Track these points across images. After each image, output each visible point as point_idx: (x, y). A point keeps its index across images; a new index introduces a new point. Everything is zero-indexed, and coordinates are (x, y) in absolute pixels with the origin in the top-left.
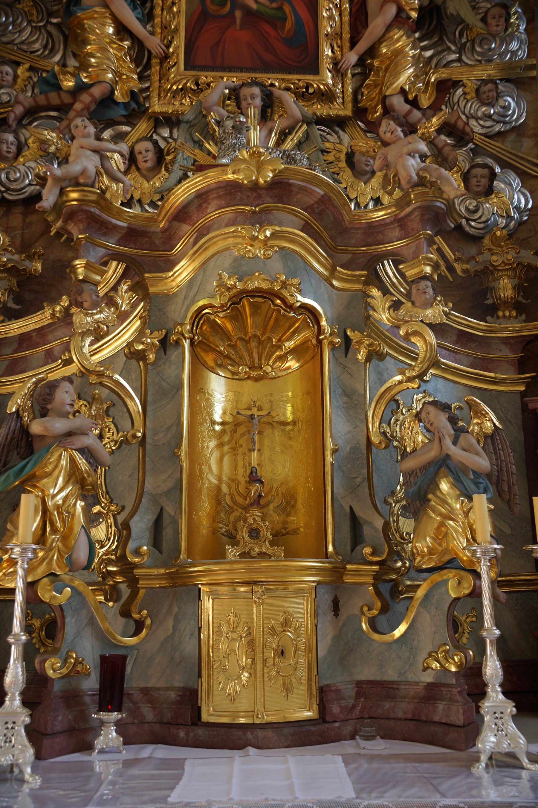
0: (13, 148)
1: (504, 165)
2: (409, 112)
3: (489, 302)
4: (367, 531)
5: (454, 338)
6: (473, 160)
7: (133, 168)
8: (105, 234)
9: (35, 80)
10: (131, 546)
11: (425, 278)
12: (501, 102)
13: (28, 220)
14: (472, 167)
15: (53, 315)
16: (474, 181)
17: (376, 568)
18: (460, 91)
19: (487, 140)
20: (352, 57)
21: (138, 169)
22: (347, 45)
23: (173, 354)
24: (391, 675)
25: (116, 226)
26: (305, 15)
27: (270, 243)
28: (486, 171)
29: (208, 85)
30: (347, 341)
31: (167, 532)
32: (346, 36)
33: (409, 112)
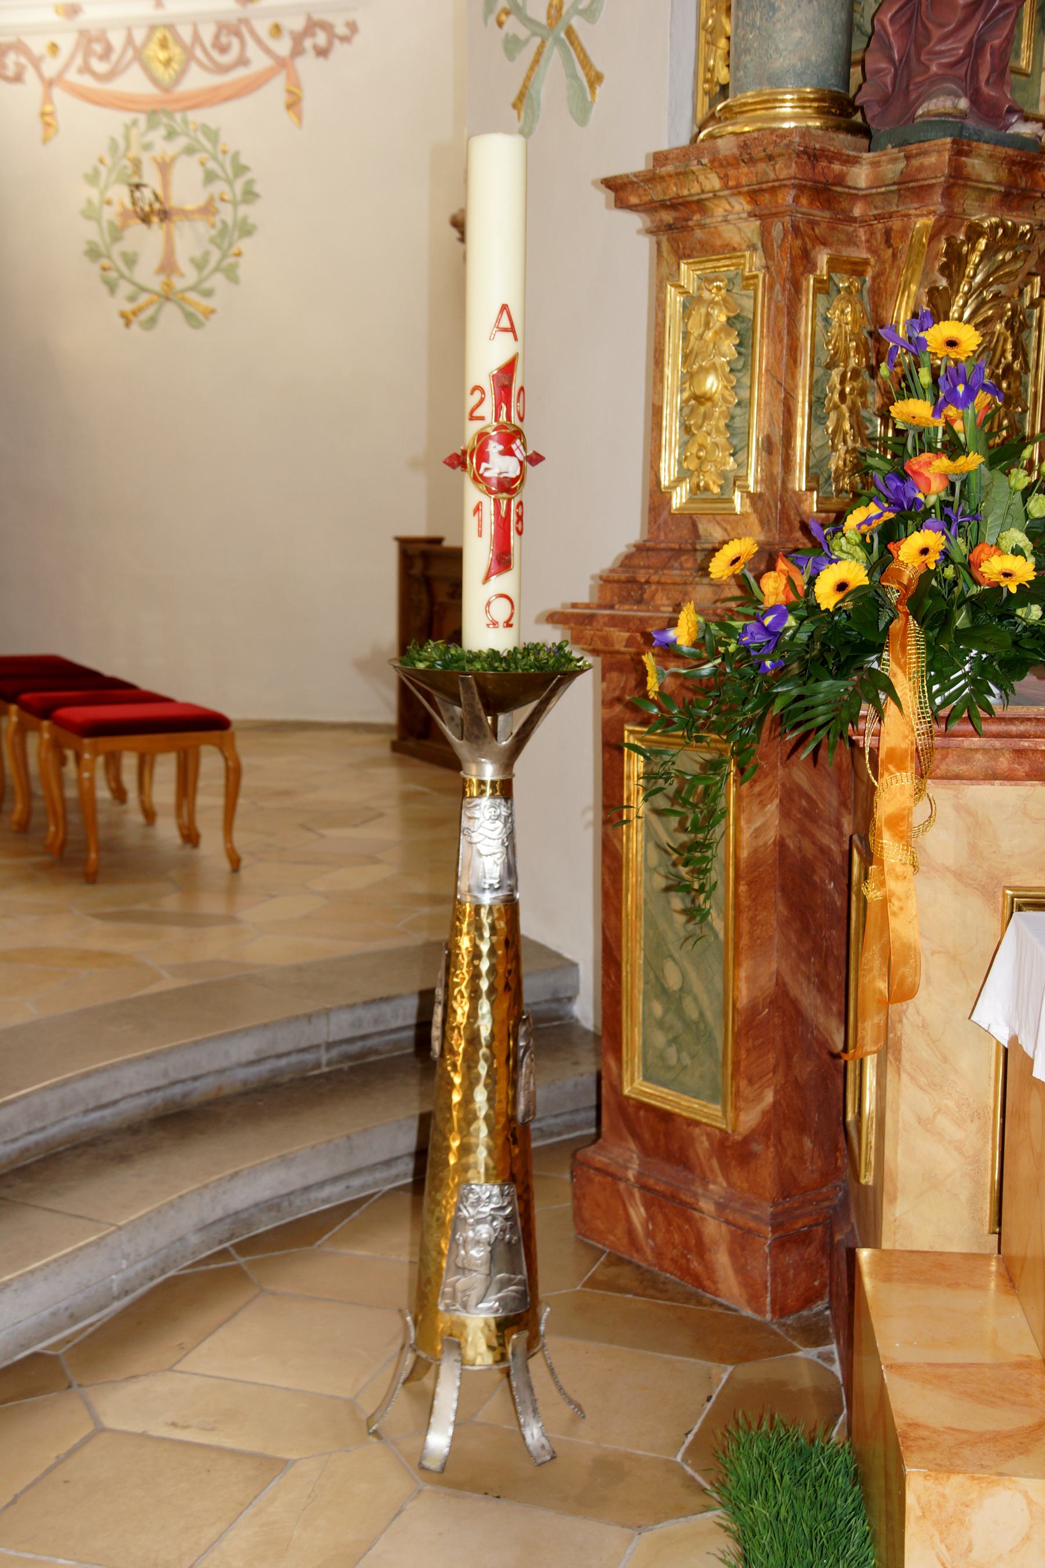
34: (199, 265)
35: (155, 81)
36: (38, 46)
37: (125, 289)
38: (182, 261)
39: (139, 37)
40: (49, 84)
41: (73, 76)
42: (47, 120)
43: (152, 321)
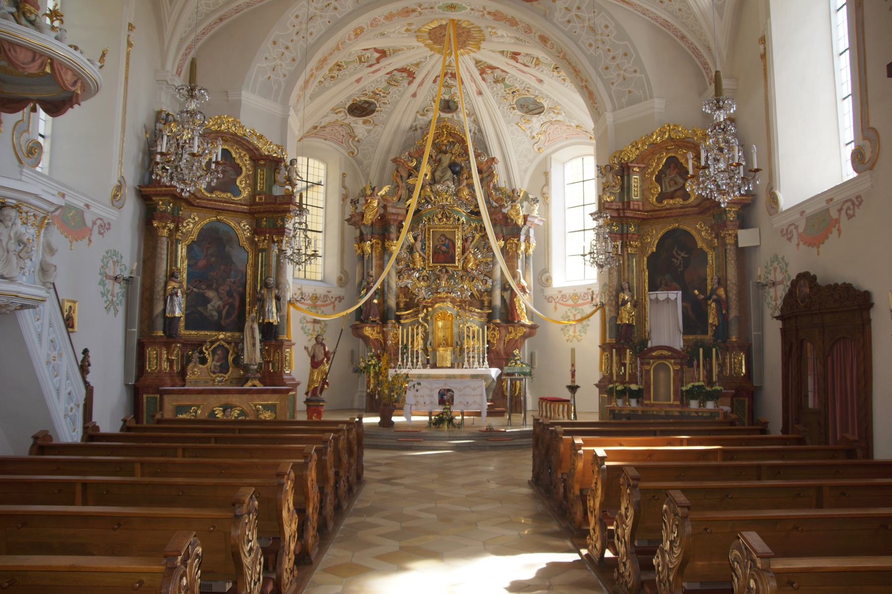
1: (490, 278)
20: (462, 259)
26: (453, 251)
34: (580, 331)
35: (574, 302)
36: (555, 297)
37: (567, 335)
38: (577, 331)
39: (571, 295)
40: (556, 303)
41: (560, 301)
42: (556, 308)
43: (572, 341)
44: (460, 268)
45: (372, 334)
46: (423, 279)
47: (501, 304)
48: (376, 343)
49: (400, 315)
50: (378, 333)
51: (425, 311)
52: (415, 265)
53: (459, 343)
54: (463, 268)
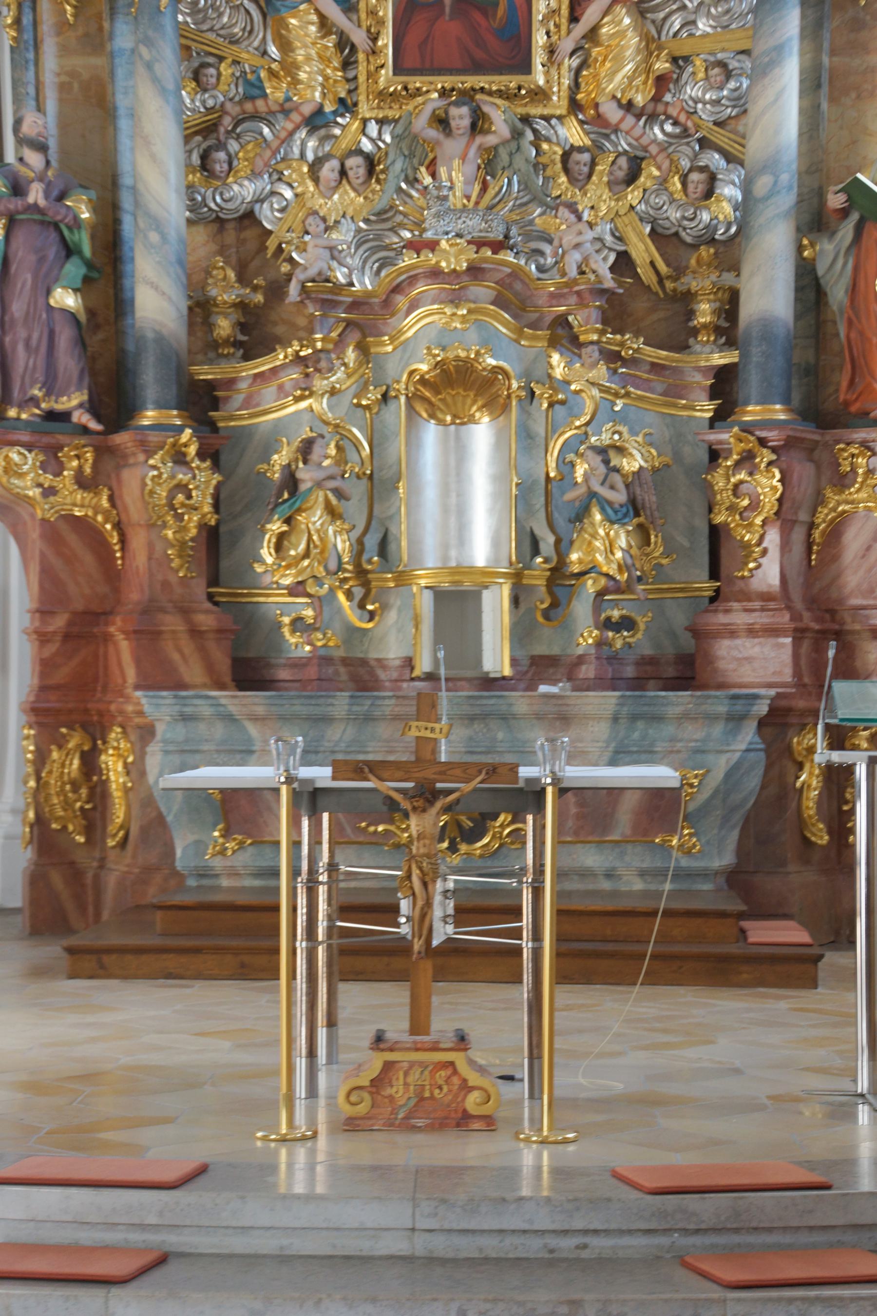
0: (226, 166)
2: (622, 120)
3: (691, 324)
4: (542, 546)
5: (648, 367)
6: (696, 155)
7: (344, 182)
8: (334, 307)
9: (238, 74)
10: (365, 557)
11: (592, 343)
12: (732, 85)
13: (242, 236)
14: (691, 170)
15: (286, 357)
16: (691, 187)
17: (548, 573)
18: (690, 69)
19: (716, 128)
20: (567, 45)
21: (349, 182)
22: (564, 21)
23: (392, 405)
24: (555, 651)
25: (341, 302)
27: (468, 317)
28: (702, 177)
29: (418, 89)
30: (533, 393)
31: (392, 547)
32: (565, 11)
33: (622, 120)
44: (559, 103)
45: (49, 492)
46: (343, 173)
47: (798, 317)
48: (73, 539)
49: (211, 386)
50: (82, 482)
51: (351, 355)
52: (296, 82)
53: (548, 541)
54: (575, 106)
